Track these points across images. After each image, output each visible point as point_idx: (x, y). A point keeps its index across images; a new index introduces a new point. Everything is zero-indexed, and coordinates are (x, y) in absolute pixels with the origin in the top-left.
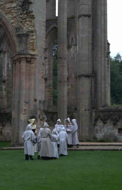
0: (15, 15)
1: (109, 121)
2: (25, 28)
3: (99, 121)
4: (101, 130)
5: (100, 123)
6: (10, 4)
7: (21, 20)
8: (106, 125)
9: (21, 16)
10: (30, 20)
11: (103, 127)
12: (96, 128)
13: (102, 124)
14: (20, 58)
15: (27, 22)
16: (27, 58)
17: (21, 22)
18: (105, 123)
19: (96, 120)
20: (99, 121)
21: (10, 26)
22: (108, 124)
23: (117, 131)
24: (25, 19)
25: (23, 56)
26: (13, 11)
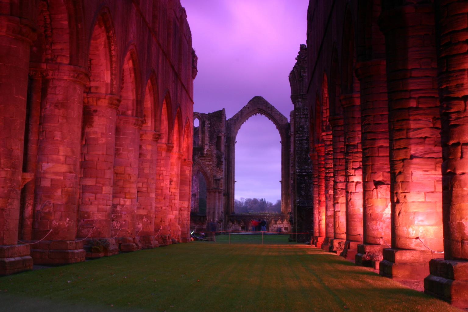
0: (210, 168)
1: (236, 222)
2: (218, 176)
3: (230, 222)
4: (230, 227)
6: (208, 163)
7: (216, 172)
8: (234, 224)
9: (216, 170)
10: (221, 172)
11: (232, 226)
12: (228, 226)
13: (231, 224)
14: (215, 191)
15: (219, 173)
16: (219, 191)
17: (216, 173)
18: (233, 223)
19: (228, 221)
20: (230, 222)
21: (208, 174)
22: (235, 224)
23: (240, 228)
24: (218, 172)
25: (218, 190)
26: (209, 166)
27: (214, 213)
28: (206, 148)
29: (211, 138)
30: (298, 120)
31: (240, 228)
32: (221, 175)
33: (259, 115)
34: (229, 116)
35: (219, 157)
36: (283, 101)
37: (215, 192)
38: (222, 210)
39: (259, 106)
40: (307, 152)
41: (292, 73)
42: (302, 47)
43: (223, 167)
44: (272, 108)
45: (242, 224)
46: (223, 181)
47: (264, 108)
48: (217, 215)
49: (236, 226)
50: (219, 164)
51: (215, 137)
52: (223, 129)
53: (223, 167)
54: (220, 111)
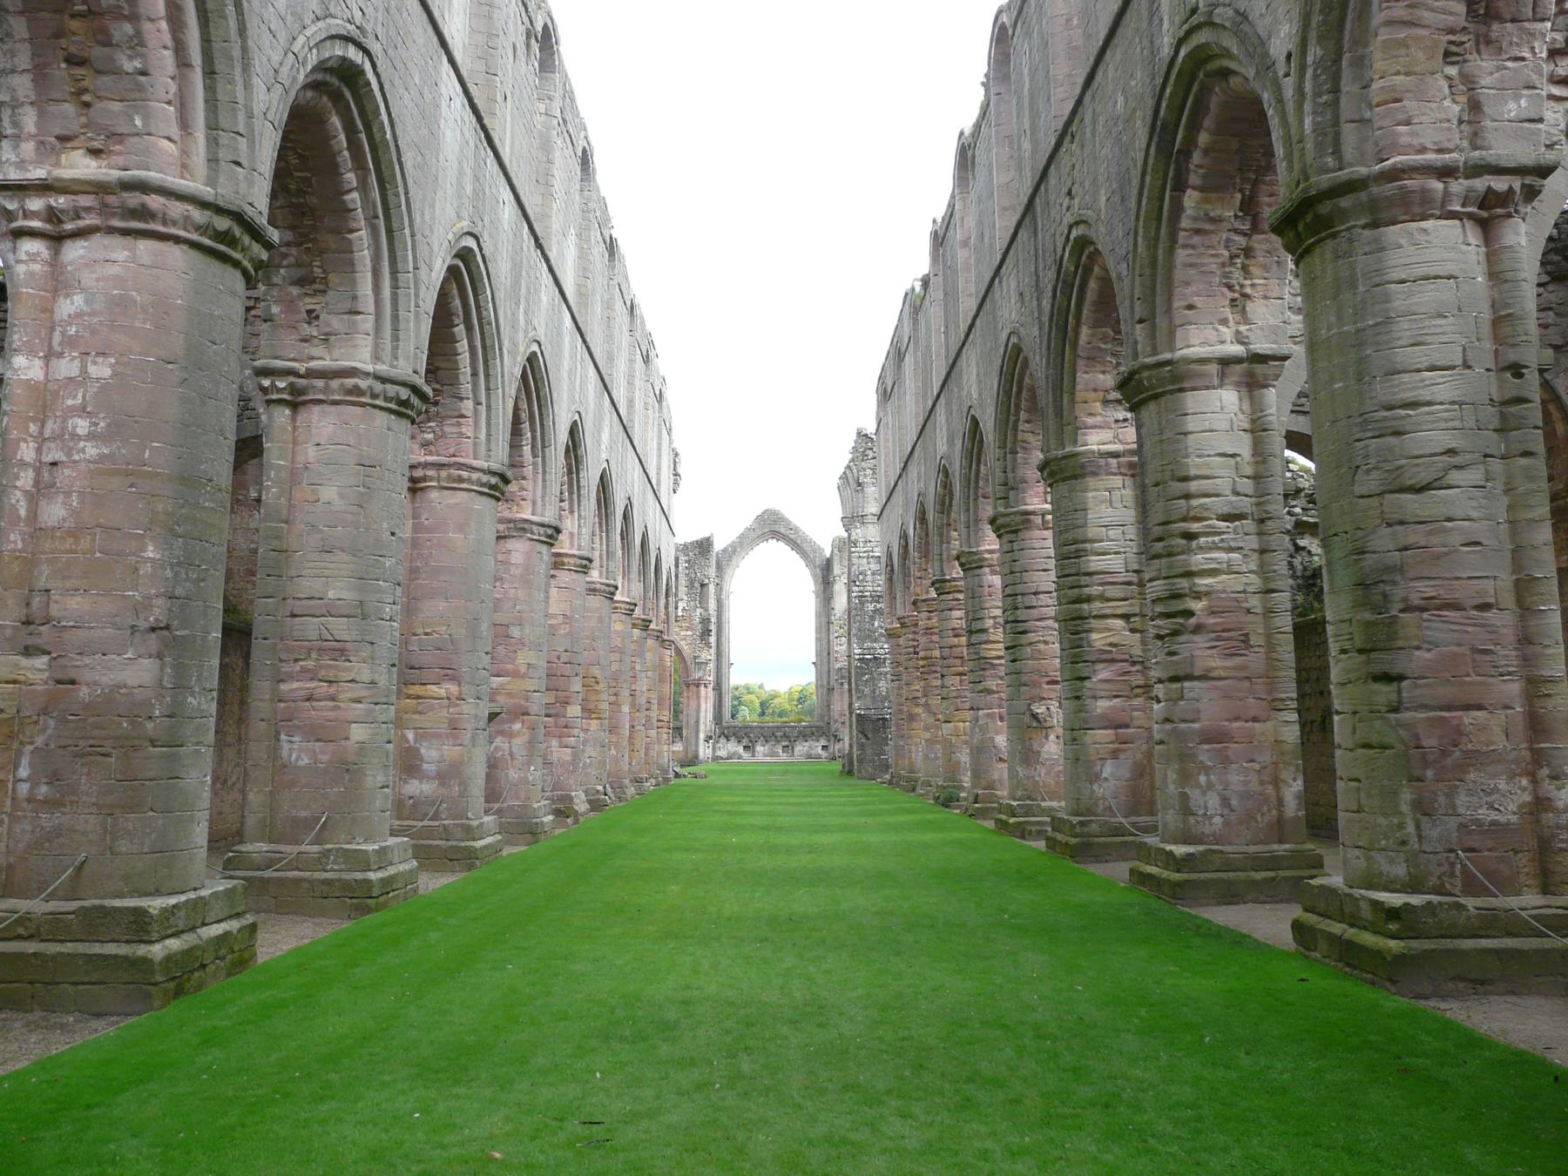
5: (723, 740)
27: (697, 722)
28: (681, 605)
29: (691, 585)
30: (855, 561)
31: (740, 749)
32: (708, 655)
33: (773, 542)
34: (718, 546)
35: (705, 621)
36: (823, 524)
37: (698, 686)
38: (710, 716)
39: (772, 527)
40: (873, 618)
41: (844, 477)
42: (862, 436)
43: (713, 640)
44: (796, 530)
45: (745, 742)
46: (712, 666)
47: (782, 530)
48: (702, 727)
49: (733, 747)
50: (706, 633)
51: (697, 585)
52: (712, 572)
53: (713, 640)
54: (708, 539)
